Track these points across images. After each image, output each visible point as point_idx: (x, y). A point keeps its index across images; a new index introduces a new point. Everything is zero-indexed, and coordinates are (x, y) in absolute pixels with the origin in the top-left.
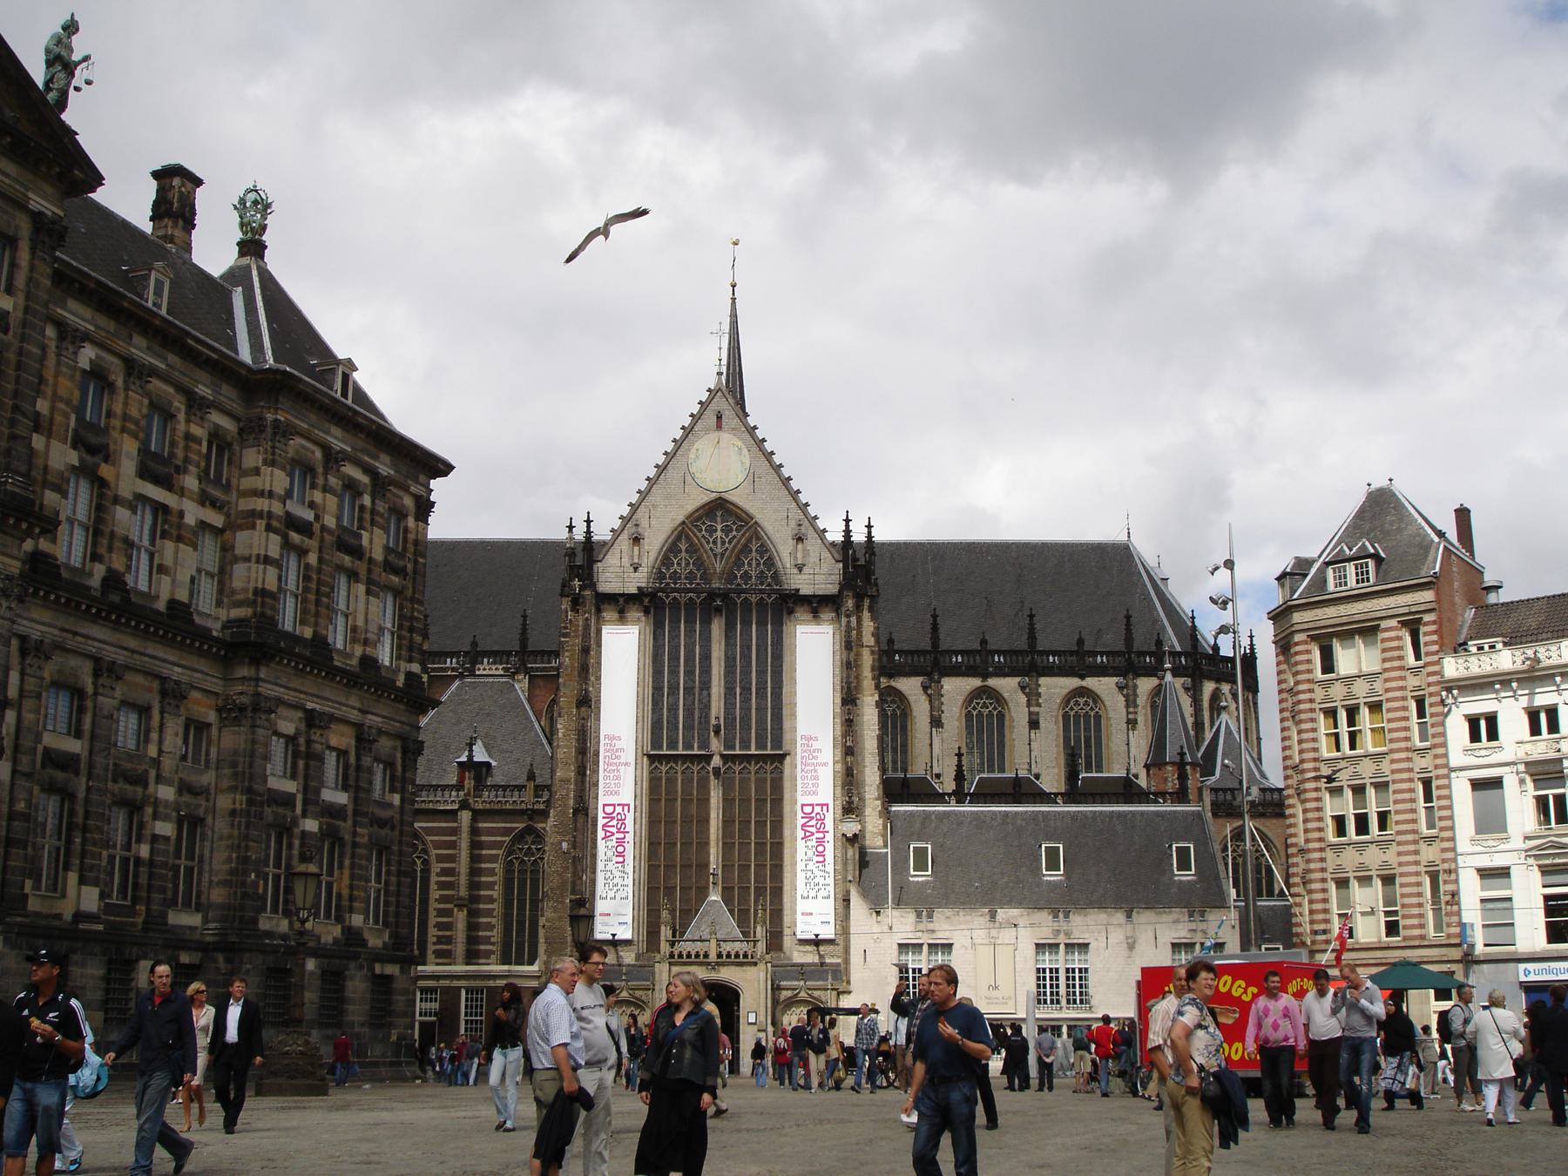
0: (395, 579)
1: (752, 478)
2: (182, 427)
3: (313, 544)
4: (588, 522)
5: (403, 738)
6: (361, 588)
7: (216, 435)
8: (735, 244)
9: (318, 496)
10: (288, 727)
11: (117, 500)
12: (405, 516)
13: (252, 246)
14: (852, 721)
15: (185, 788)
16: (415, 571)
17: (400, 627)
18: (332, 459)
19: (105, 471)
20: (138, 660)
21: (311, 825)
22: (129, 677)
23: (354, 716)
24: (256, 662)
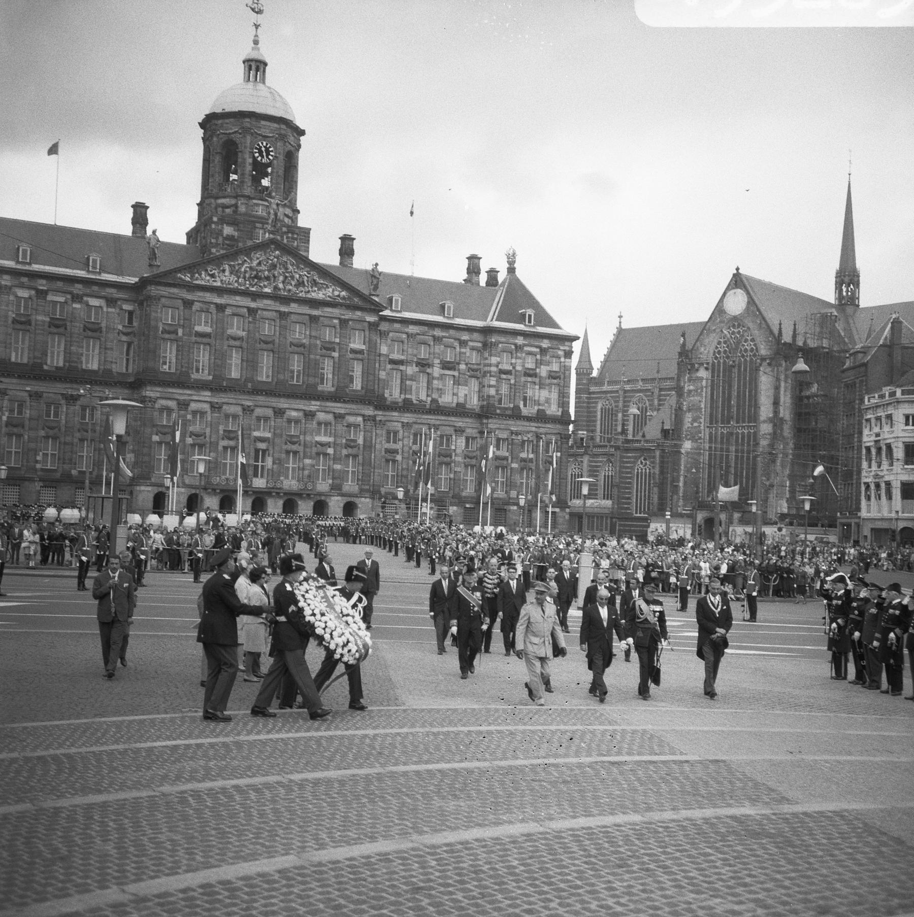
0: (555, 381)
1: (747, 308)
2: (458, 349)
3: (512, 377)
6: (537, 387)
7: (473, 349)
9: (513, 361)
10: (505, 436)
11: (433, 378)
13: (511, 270)
15: (466, 457)
16: (564, 378)
18: (519, 348)
19: (429, 370)
20: (447, 423)
21: (515, 465)
22: (444, 428)
23: (534, 429)
24: (487, 418)
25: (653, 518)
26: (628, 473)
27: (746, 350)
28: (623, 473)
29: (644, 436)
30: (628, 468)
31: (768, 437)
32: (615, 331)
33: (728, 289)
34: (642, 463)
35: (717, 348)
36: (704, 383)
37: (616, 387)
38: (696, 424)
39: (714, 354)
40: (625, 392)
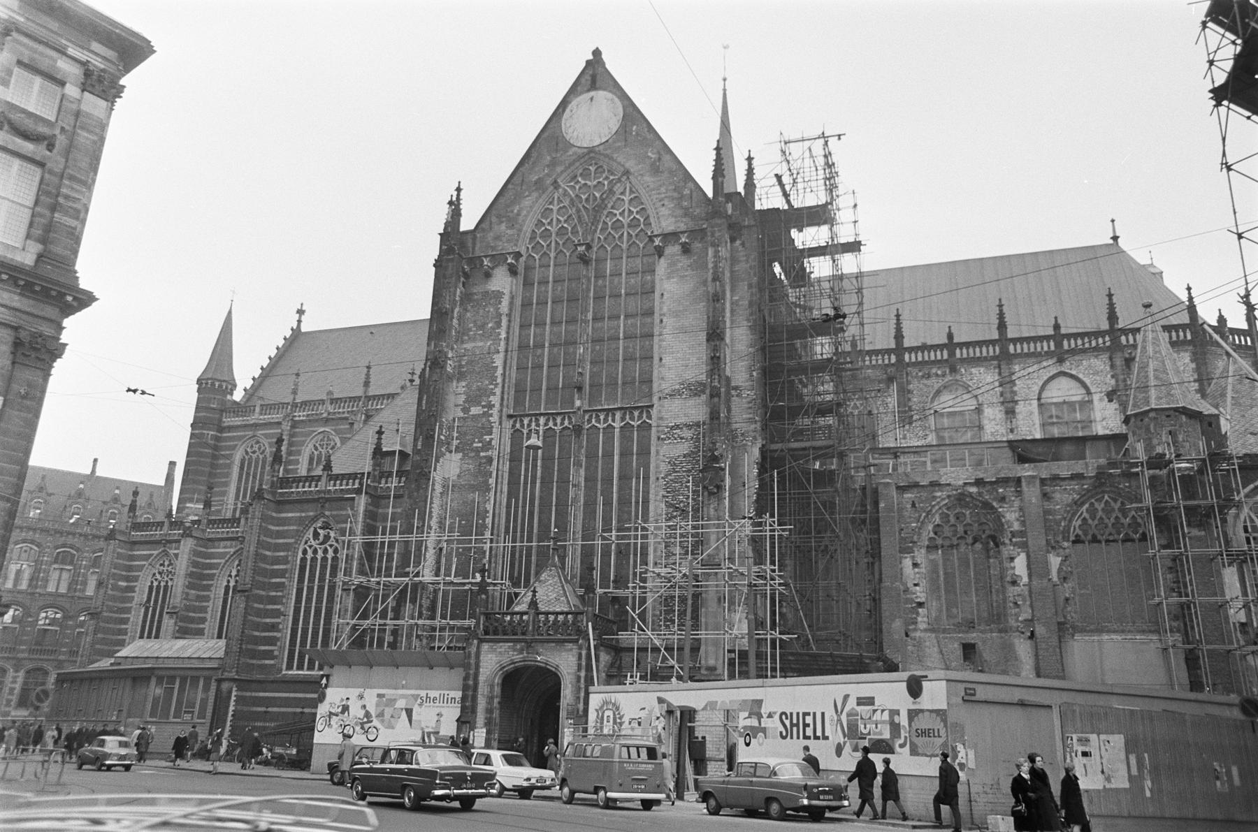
0: (28, 147)
4: (459, 190)
5: (16, 329)
8: (726, 47)
12: (62, 84)
14: (719, 358)
17: (36, 203)
25: (338, 673)
26: (277, 561)
27: (618, 225)
28: (264, 559)
29: (328, 467)
30: (277, 547)
31: (687, 434)
32: (288, 334)
33: (574, 91)
34: (316, 535)
35: (540, 223)
36: (504, 306)
37: (276, 417)
38: (475, 410)
39: (532, 238)
40: (295, 424)
